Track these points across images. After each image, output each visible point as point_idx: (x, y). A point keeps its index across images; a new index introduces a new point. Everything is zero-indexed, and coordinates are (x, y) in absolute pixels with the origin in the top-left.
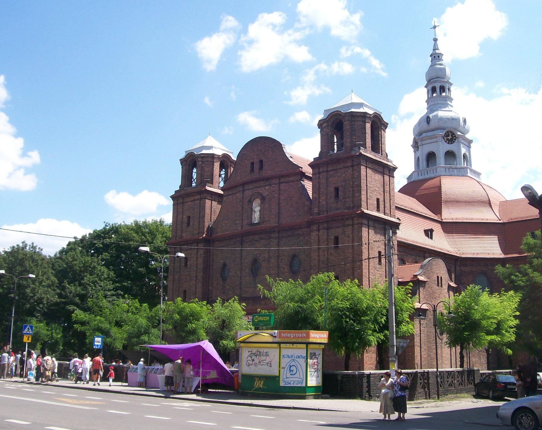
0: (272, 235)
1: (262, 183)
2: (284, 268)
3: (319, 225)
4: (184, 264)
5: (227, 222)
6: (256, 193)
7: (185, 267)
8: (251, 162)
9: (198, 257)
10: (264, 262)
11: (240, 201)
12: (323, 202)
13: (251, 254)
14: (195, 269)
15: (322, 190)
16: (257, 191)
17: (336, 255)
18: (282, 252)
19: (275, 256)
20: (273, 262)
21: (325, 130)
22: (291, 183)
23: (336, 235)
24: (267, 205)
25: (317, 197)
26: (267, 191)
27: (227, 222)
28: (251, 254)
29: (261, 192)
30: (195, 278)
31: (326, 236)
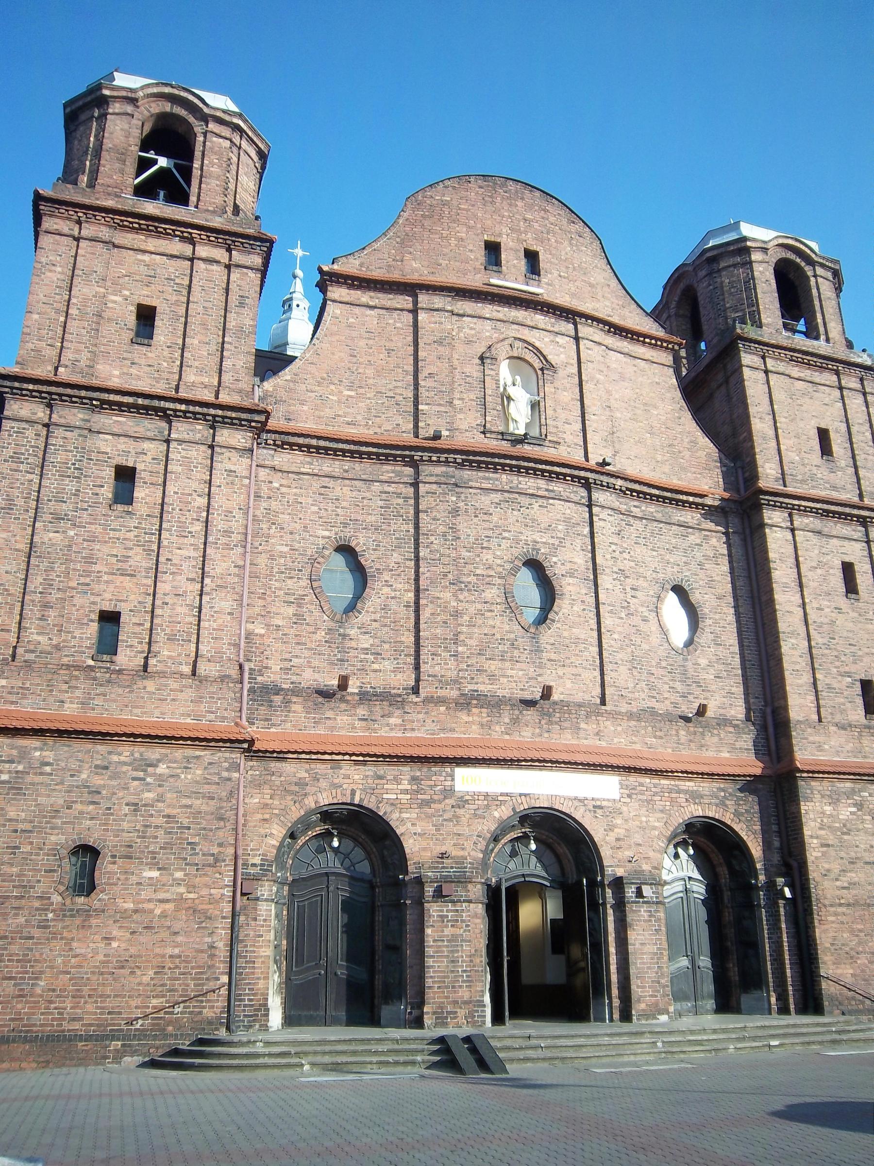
0: (599, 496)
1: (540, 319)
2: (645, 620)
3: (790, 515)
4: (107, 492)
5: (352, 393)
6: (520, 339)
7: (120, 507)
8: (486, 238)
9: (216, 481)
10: (571, 580)
11: (440, 342)
12: (790, 453)
13: (506, 534)
14: (198, 527)
15: (783, 420)
16: (519, 336)
17: (856, 615)
18: (633, 564)
19: (615, 569)
20: (610, 586)
21: (761, 269)
22: (642, 364)
23: (847, 559)
24: (565, 393)
25: (772, 433)
26: (562, 350)
27: (352, 393)
28: (506, 534)
29: (537, 344)
30: (190, 569)
31: (816, 552)
